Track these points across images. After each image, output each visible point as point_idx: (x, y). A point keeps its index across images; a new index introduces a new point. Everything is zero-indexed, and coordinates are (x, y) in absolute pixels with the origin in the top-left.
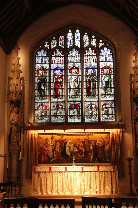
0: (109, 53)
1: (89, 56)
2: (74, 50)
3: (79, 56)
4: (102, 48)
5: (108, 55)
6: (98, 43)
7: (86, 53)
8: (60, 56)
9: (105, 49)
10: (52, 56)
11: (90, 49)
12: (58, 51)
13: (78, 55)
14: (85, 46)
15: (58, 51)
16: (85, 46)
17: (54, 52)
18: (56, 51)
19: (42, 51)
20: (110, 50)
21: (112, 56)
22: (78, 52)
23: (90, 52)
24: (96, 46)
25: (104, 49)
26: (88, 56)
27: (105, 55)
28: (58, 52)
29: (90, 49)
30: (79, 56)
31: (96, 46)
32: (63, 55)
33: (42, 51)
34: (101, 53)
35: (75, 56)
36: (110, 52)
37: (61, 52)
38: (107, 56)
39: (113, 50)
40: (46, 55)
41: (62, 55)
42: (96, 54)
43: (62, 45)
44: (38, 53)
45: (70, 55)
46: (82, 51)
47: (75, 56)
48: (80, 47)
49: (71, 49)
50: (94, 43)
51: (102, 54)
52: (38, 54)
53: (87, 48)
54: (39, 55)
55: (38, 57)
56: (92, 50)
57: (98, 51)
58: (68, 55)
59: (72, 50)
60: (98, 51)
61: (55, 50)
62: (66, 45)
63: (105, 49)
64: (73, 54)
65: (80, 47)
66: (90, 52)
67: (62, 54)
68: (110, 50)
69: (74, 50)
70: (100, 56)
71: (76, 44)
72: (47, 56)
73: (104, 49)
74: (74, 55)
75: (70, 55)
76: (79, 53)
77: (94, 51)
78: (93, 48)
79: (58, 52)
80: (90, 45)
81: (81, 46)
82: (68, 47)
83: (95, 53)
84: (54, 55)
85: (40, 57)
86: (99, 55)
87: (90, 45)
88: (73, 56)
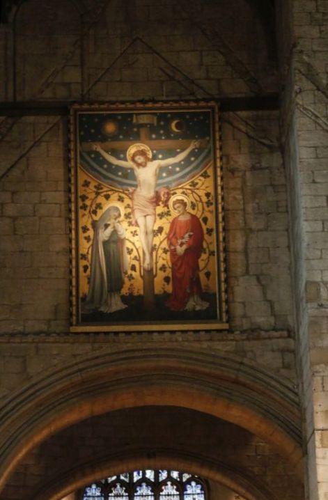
0: (199, 491)
1: (168, 495)
2: (144, 484)
3: (151, 495)
4: (189, 482)
5: (198, 494)
6: (181, 476)
7: (162, 491)
8: (123, 496)
9: (193, 484)
10: (110, 495)
11: (169, 483)
12: (118, 487)
13: (150, 493)
14: (161, 479)
15: (118, 487)
16: (161, 479)
17: (113, 489)
18: (115, 487)
19: (94, 487)
20: (199, 486)
21: (203, 495)
22: (150, 489)
23: (170, 489)
24: (178, 480)
25: (190, 485)
26: (165, 495)
27: (193, 494)
28: (119, 489)
29: (169, 483)
30: (151, 495)
31: (178, 480)
32: (127, 494)
33: (94, 487)
34: (186, 490)
35: (145, 496)
36: (201, 490)
37: (124, 488)
38: (196, 496)
39: (205, 486)
40: (99, 494)
41: (125, 494)
42: (178, 493)
43: (126, 477)
44: (88, 490)
45: (138, 493)
46: (156, 487)
47: (145, 496)
48: (153, 480)
49: (139, 483)
50: (175, 475)
51: (189, 491)
52: (86, 493)
53: (164, 483)
54: (88, 494)
55: (87, 496)
56: (172, 485)
57: (181, 487)
58: (136, 494)
59: (141, 486)
60: (181, 487)
61: (114, 484)
62: (131, 478)
63: (193, 484)
64: (142, 491)
65: (153, 480)
66: (170, 489)
67: (125, 491)
68: (199, 486)
69: (144, 484)
70: (185, 496)
71: (147, 476)
72: (101, 496)
73: (190, 485)
74: (144, 494)
75: (138, 493)
76: (152, 491)
77: (175, 487)
78: (174, 482)
79: (119, 489)
80: (169, 478)
81: (155, 479)
82: (135, 479)
83: (177, 490)
84: (112, 494)
85: (89, 496)
86: (184, 495)
87: (169, 478)
88: (143, 496)
